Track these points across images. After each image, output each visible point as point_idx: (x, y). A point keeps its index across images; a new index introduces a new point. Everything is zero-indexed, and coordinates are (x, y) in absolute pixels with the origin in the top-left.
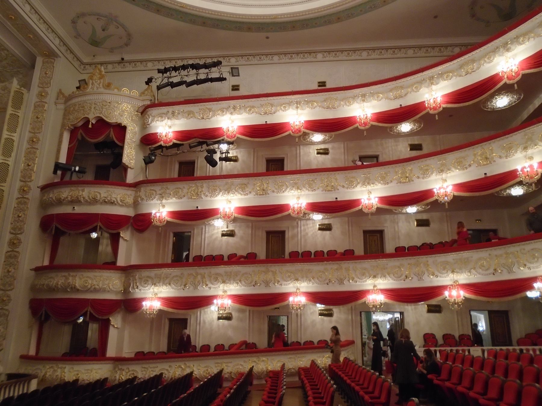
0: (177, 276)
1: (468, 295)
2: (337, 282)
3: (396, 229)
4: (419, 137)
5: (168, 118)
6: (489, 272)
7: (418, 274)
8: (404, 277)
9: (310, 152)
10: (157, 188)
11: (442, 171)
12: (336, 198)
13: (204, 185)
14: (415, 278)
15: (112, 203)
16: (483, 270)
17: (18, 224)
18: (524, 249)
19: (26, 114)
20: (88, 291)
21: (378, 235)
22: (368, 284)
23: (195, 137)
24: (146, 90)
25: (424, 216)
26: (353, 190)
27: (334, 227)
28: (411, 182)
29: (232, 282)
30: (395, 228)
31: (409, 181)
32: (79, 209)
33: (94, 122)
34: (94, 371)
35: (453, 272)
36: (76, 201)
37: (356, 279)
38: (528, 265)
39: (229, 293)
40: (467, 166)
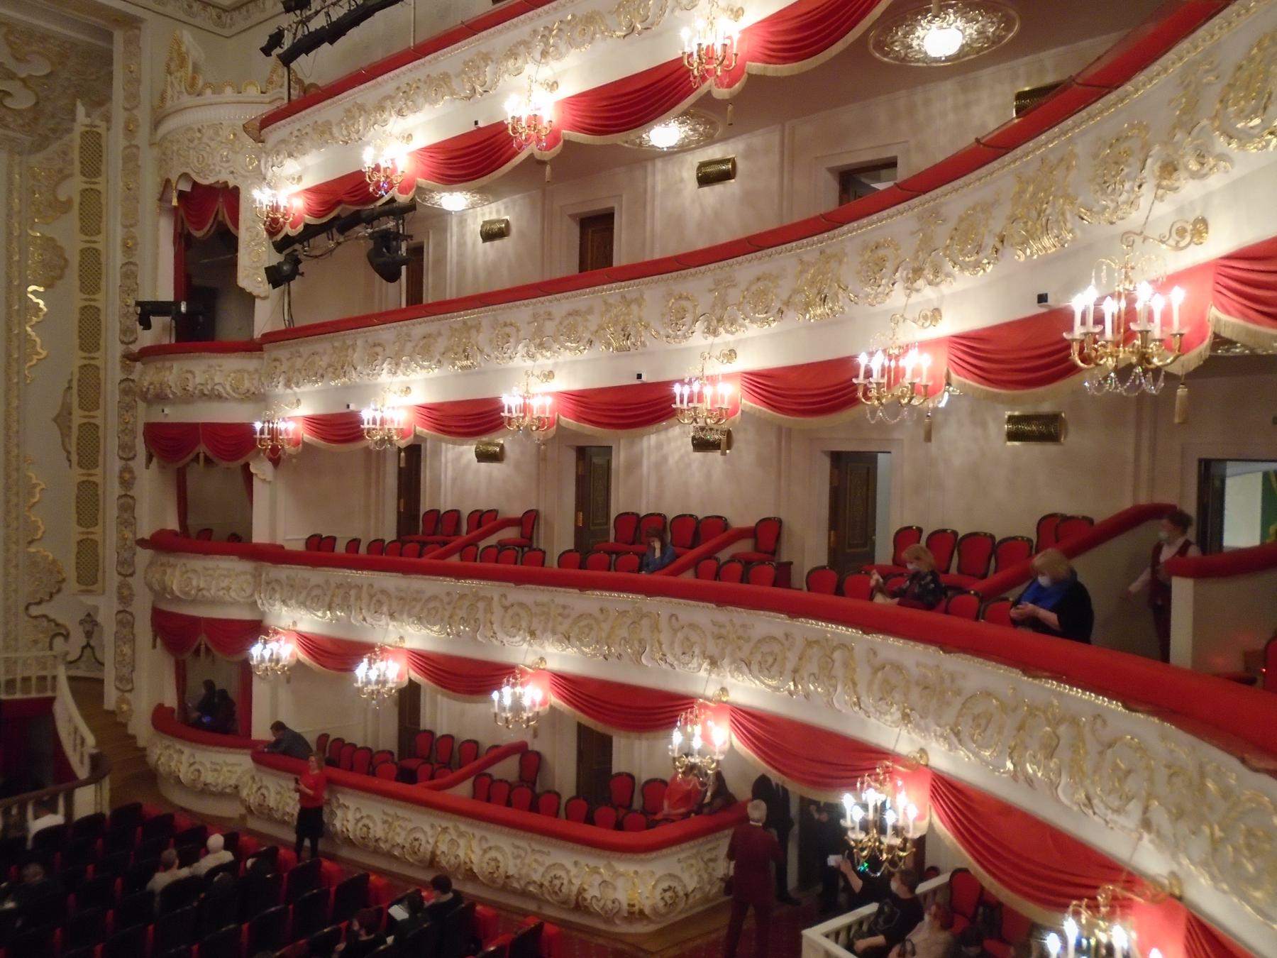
0: (318, 586)
4: (1062, 49)
5: (290, 155)
9: (682, 180)
10: (282, 352)
13: (359, 343)
15: (219, 397)
17: (126, 438)
19: (112, 182)
20: (194, 602)
22: (703, 681)
23: (339, 203)
24: (274, 71)
26: (684, 344)
29: (405, 616)
32: (173, 414)
33: (186, 187)
34: (225, 769)
36: (161, 398)
37: (670, 658)
39: (408, 644)
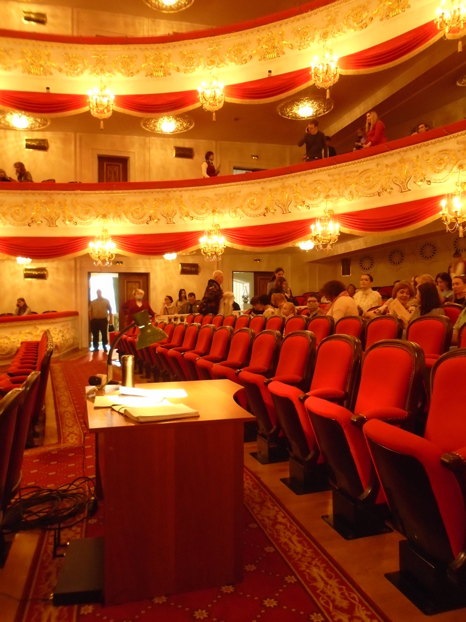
1: (229, 244)
2: (45, 222)
3: (147, 158)
6: (258, 212)
7: (167, 214)
8: (146, 218)
11: (212, 62)
12: (48, 88)
14: (163, 220)
16: (252, 209)
18: (305, 181)
21: (121, 165)
25: (186, 143)
26: (76, 79)
27: (53, 146)
28: (168, 77)
30: (144, 155)
31: (165, 75)
35: (214, 211)
38: (308, 202)
40: (247, 57)
